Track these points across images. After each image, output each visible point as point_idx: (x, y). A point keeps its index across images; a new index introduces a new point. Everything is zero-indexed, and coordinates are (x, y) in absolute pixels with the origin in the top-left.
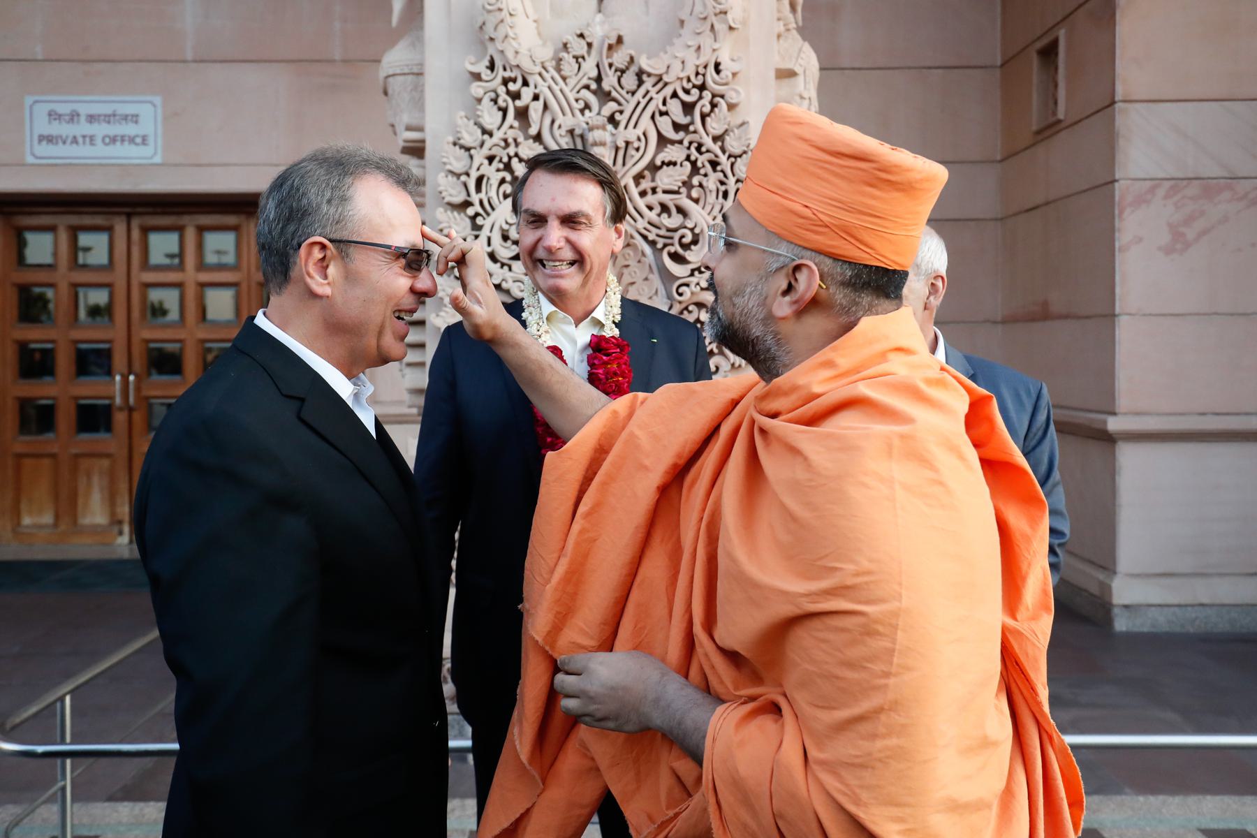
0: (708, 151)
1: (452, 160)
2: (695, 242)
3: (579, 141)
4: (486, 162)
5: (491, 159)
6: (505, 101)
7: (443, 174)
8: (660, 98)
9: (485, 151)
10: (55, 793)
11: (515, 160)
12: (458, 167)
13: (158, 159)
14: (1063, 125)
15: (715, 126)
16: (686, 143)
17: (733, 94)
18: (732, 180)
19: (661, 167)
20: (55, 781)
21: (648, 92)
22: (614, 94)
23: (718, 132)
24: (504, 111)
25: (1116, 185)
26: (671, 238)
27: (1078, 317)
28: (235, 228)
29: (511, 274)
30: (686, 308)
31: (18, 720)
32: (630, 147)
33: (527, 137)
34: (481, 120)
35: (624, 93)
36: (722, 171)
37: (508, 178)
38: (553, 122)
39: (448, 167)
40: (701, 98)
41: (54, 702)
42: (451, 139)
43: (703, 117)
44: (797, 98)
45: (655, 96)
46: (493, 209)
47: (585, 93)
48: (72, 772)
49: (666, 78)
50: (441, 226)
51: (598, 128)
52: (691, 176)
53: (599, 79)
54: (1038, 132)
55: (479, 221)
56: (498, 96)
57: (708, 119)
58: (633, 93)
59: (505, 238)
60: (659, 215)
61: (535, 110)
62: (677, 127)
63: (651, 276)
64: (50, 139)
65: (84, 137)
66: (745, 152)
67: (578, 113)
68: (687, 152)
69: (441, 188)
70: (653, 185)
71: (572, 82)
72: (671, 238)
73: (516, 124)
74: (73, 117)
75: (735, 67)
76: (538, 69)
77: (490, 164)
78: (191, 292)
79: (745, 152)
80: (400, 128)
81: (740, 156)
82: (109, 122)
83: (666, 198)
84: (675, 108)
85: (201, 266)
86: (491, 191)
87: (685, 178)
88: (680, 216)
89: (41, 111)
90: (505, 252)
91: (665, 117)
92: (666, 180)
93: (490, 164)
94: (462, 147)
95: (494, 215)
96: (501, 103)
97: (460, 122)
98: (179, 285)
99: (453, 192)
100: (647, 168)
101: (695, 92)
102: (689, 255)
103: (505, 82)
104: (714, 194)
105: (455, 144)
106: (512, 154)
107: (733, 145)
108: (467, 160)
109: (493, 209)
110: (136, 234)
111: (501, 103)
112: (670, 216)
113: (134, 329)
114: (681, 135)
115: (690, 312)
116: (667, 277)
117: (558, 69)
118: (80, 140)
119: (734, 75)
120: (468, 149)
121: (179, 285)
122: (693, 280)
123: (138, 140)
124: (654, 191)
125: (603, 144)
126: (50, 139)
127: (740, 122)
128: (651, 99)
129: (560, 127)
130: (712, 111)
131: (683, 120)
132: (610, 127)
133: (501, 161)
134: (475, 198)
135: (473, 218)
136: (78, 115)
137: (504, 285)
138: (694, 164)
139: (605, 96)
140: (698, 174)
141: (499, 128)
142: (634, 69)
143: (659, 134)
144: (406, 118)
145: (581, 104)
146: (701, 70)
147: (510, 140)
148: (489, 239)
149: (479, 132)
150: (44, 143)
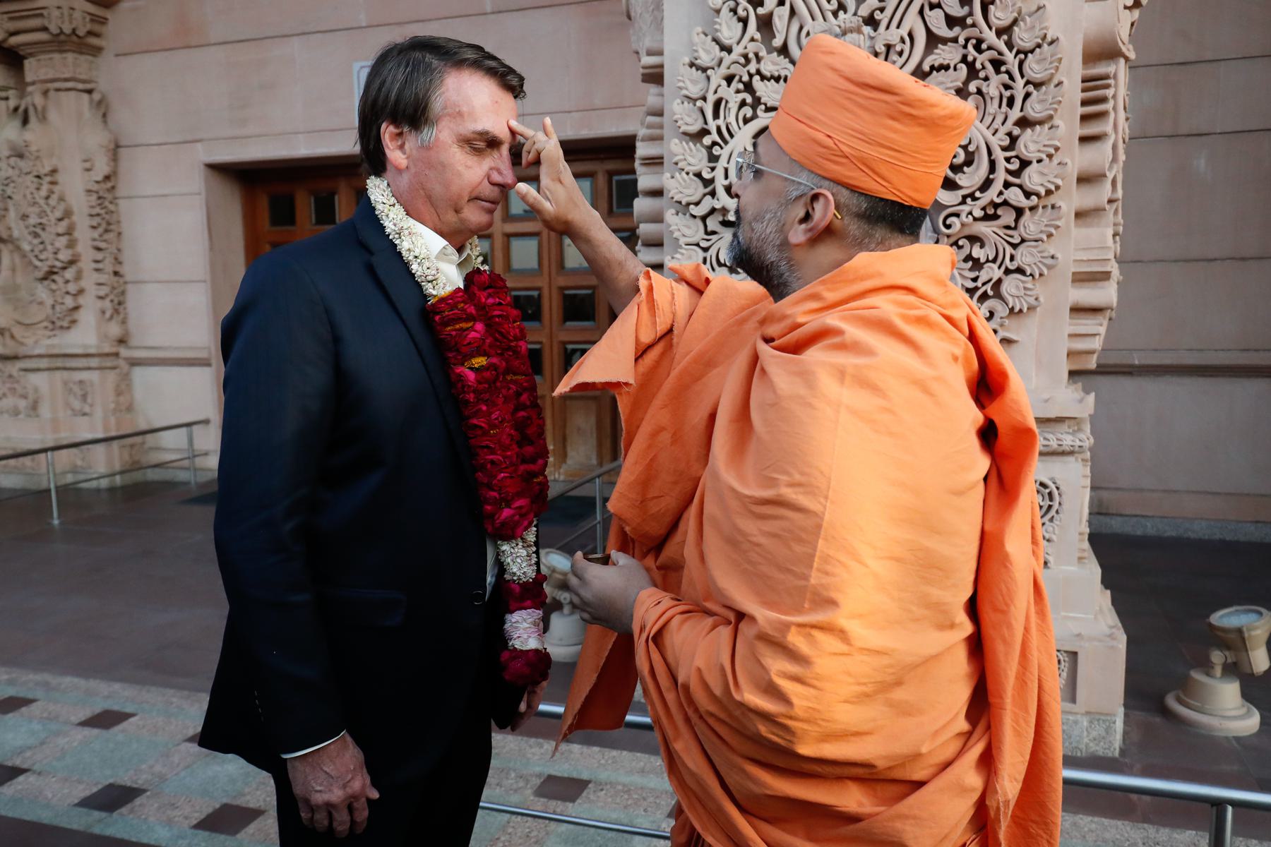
0: (990, 48)
2: (969, 162)
4: (724, 83)
5: (729, 79)
6: (746, 9)
7: (679, 101)
9: (723, 71)
11: (757, 78)
12: (694, 91)
15: (1000, 15)
16: (961, 40)
18: (1020, 82)
24: (744, 21)
33: (770, 50)
36: (1008, 72)
37: (749, 100)
38: (801, 28)
39: (685, 92)
42: (687, 60)
50: (676, 159)
52: (966, 83)
57: (992, 7)
61: (781, 18)
62: (951, 21)
66: (1039, 46)
67: (830, 16)
68: (964, 51)
69: (676, 117)
73: (758, 36)
77: (729, 86)
79: (1039, 46)
80: (643, 53)
81: (1032, 51)
86: (730, 116)
91: (938, 12)
93: (729, 86)
94: (698, 68)
95: (732, 143)
97: (696, 39)
99: (688, 120)
102: (960, 179)
104: (996, 102)
105: (692, 65)
106: (753, 71)
107: (1023, 37)
108: (703, 84)
111: (741, 12)
114: (957, 29)
115: (960, 247)
120: (704, 70)
122: (966, 208)
127: (1035, 8)
129: (808, 34)
131: (958, 11)
132: (867, 30)
134: (712, 125)
135: (709, 148)
138: (971, 66)
140: (978, 78)
144: (648, 43)
147: (751, 55)
148: (726, 170)
149: (717, 47)
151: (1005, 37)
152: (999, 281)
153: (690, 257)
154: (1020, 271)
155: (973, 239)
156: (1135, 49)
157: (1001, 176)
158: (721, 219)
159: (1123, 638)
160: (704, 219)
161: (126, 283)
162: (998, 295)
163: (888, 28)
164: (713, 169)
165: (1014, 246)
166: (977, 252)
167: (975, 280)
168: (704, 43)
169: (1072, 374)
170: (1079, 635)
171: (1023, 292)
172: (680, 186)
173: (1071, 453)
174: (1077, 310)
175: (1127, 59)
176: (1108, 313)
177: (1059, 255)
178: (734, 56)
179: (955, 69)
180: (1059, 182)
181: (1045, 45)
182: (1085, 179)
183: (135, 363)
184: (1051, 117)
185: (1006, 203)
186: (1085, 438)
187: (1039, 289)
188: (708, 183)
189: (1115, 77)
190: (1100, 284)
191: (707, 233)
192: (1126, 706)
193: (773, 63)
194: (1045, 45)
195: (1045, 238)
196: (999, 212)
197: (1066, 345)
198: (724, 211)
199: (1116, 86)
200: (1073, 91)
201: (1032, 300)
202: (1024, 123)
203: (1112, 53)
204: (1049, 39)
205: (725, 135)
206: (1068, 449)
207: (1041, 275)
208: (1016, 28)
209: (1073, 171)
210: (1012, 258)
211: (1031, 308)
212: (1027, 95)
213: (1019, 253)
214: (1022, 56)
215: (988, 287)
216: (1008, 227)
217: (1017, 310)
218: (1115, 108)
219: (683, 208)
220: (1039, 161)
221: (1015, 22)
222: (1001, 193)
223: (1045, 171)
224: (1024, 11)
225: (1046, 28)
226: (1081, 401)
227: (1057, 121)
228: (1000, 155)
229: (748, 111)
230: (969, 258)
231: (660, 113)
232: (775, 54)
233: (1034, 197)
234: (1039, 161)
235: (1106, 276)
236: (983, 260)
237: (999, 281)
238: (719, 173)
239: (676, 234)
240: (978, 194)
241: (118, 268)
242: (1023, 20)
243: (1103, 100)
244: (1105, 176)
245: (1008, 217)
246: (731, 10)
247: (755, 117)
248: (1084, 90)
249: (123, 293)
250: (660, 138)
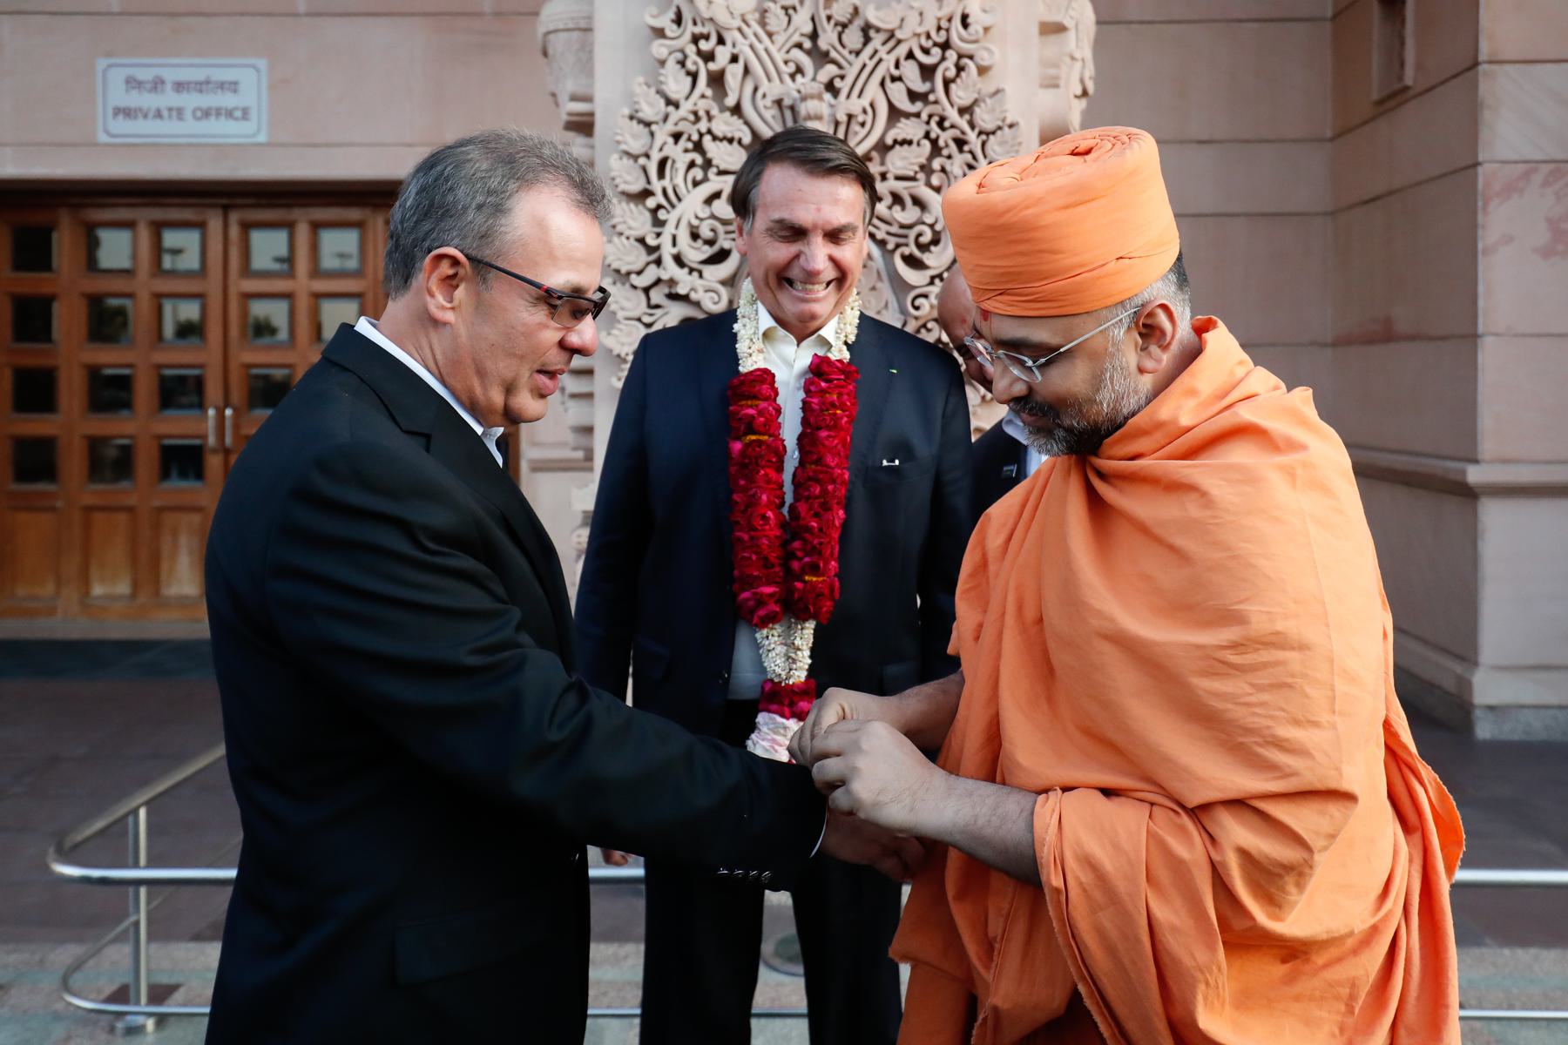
0: (952, 126)
1: (628, 138)
2: (936, 241)
3: (788, 114)
4: (671, 140)
5: (677, 137)
6: (695, 63)
8: (891, 59)
9: (670, 127)
10: (126, 931)
11: (707, 139)
12: (636, 146)
13: (262, 138)
14: (1411, 93)
15: (962, 95)
16: (924, 116)
17: (985, 54)
19: (892, 147)
20: (127, 915)
21: (876, 52)
22: (833, 54)
23: (966, 102)
24: (694, 76)
25: (1480, 170)
26: (906, 236)
27: (1431, 338)
28: (359, 225)
29: (700, 282)
30: (924, 326)
31: (79, 837)
33: (723, 109)
34: (664, 87)
35: (845, 52)
36: (971, 152)
38: (756, 89)
39: (623, 147)
40: (943, 59)
41: (126, 816)
42: (627, 112)
43: (947, 83)
44: (1067, 59)
45: (884, 56)
46: (679, 200)
47: (797, 53)
48: (148, 903)
49: (899, 35)
51: (812, 97)
53: (814, 36)
54: (1381, 102)
55: (662, 215)
56: (686, 57)
57: (953, 86)
58: (858, 53)
59: (695, 236)
60: (890, 208)
61: (733, 75)
62: (913, 96)
63: (879, 285)
64: (127, 113)
65: (170, 109)
66: (1000, 128)
67: (787, 79)
68: (925, 127)
69: (613, 174)
70: (882, 169)
71: (780, 39)
72: (906, 236)
73: (709, 92)
74: (157, 85)
75: (987, 20)
76: (737, 23)
78: (303, 304)
79: (1000, 128)
80: (563, 97)
81: (993, 133)
82: (201, 91)
83: (900, 186)
84: (911, 72)
85: (316, 272)
86: (678, 177)
87: (923, 160)
89: (117, 77)
90: (695, 254)
91: (898, 84)
92: (899, 163)
94: (640, 121)
95: (680, 207)
96: (690, 66)
98: (288, 296)
99: (629, 178)
101: (936, 51)
102: (927, 258)
103: (696, 39)
105: (631, 118)
106: (704, 130)
107: (985, 118)
108: (646, 139)
109: (679, 200)
110: (234, 231)
111: (690, 66)
112: (903, 208)
113: (233, 350)
114: (918, 106)
115: (929, 330)
116: (900, 286)
117: (763, 24)
118: (165, 113)
119: (986, 29)
120: (648, 124)
121: (288, 296)
123: (238, 114)
125: (819, 118)
126: (127, 113)
127: (992, 89)
128: (880, 60)
130: (958, 75)
131: (920, 87)
132: (828, 96)
133: (689, 139)
134: (657, 186)
136: (163, 82)
137: (693, 296)
138: (934, 142)
139: (821, 58)
140: (939, 154)
141: (687, 98)
142: (859, 23)
144: (570, 85)
145: (792, 68)
146: (944, 24)
147: (701, 113)
148: (674, 238)
149: (662, 102)
150: (121, 117)
151: (967, 117)
158: (667, 291)
160: (647, 290)
163: (848, 96)
164: (658, 235)
181: (1006, 129)
188: (651, 250)
191: (650, 306)
193: (724, 124)
194: (1006, 129)
198: (672, 282)
204: (1008, 121)
205: (673, 199)
214: (984, 137)
221: (976, 102)
229: (697, 173)
232: (728, 114)
238: (665, 240)
247: (706, 179)
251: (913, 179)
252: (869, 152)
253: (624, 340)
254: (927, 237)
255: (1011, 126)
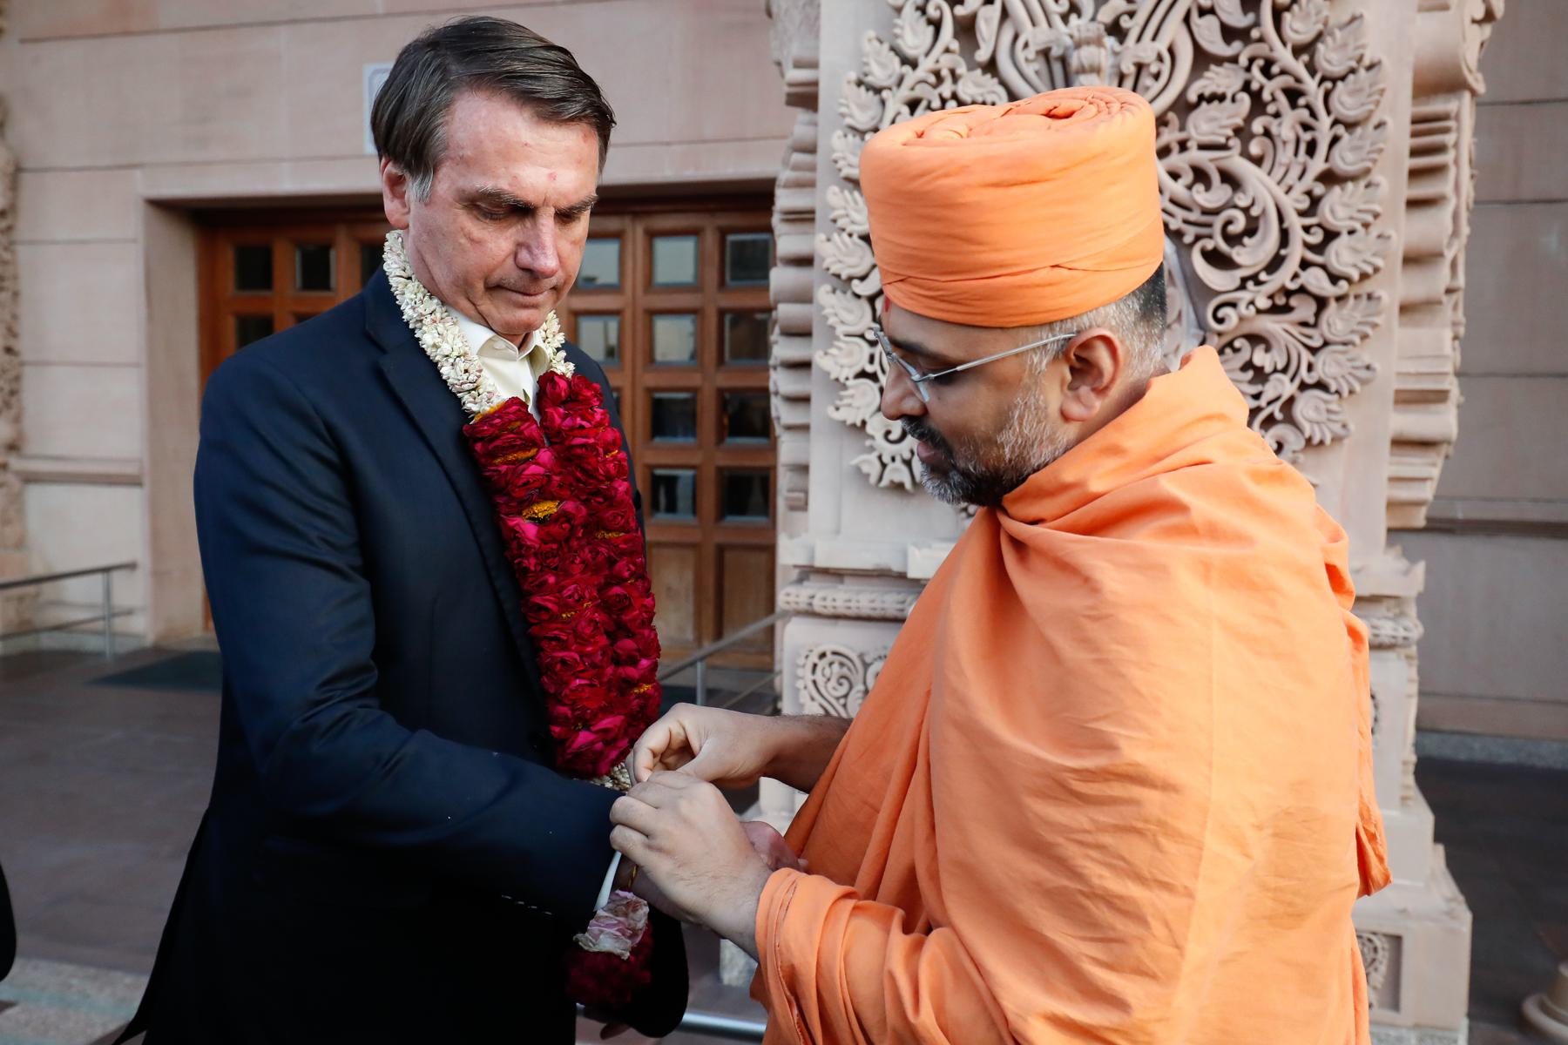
0: (1283, 72)
2: (1251, 231)
3: (1057, 68)
4: (906, 110)
6: (939, 8)
7: (840, 133)
9: (905, 93)
15: (1299, 27)
16: (1243, 61)
18: (1325, 121)
19: (1194, 107)
23: (1305, 37)
24: (937, 25)
26: (1209, 225)
30: (1230, 344)
32: (1144, 73)
34: (899, 42)
36: (1308, 107)
38: (1016, 37)
39: (849, 121)
42: (853, 76)
50: (833, 215)
51: (1088, 42)
52: (1249, 119)
57: (1287, 16)
60: (1189, 187)
62: (1229, 33)
66: (1353, 71)
67: (1057, 21)
68: (1245, 76)
69: (835, 156)
70: (1182, 136)
72: (1209, 225)
73: (955, 45)
77: (912, 112)
79: (1353, 71)
81: (1343, 78)
83: (1204, 158)
87: (1239, 121)
88: (1227, 189)
91: (1210, 20)
92: (1205, 127)
93: (912, 112)
94: (869, 88)
96: (932, 12)
97: (867, 47)
100: (1173, 107)
102: (1237, 254)
104: (1291, 148)
105: (860, 83)
106: (947, 94)
107: (1330, 58)
108: (875, 109)
111: (932, 12)
112: (1208, 187)
114: (1237, 45)
115: (1236, 350)
120: (878, 91)
122: (1244, 296)
124: (1183, 146)
125: (1096, 70)
127: (1346, 18)
129: (1026, 45)
131: (1238, 20)
132: (1110, 41)
138: (1256, 97)
140: (1264, 113)
141: (927, 54)
143: (1197, 48)
144: (795, 50)
147: (945, 73)
149: (897, 60)
151: (1305, 58)
152: (1291, 400)
153: (850, 354)
154: (1321, 386)
155: (1255, 339)
156: (1486, 80)
157: (1296, 252)
159: (1467, 917)
160: (872, 300)
161: (22, 364)
162: (1289, 419)
163: (1139, 39)
165: (1314, 351)
166: (1260, 358)
167: (1257, 397)
168: (878, 53)
169: (1390, 530)
170: (1403, 911)
171: (1324, 416)
172: (838, 252)
173: (1390, 647)
174: (1401, 443)
175: (1473, 93)
176: (1444, 449)
177: (1377, 365)
178: (921, 73)
179: (1233, 100)
180: (1379, 262)
181: (1362, 72)
182: (1414, 260)
183: (30, 479)
184: (1367, 171)
185: (1302, 290)
186: (1412, 627)
187: (1347, 412)
189: (1457, 118)
190: (1433, 407)
192: (1470, 1016)
194: (1362, 72)
195: (1356, 339)
196: (1293, 302)
197: (1385, 492)
199: (1459, 130)
200: (1399, 136)
201: (1337, 428)
202: (1329, 178)
203: (1452, 84)
204: (1367, 62)
206: (1387, 641)
207: (1351, 392)
208: (1320, 47)
209: (1398, 247)
210: (1310, 367)
211: (1337, 439)
212: (1335, 140)
213: (1320, 360)
214: (1329, 85)
215: (1275, 409)
216: (1304, 324)
217: (1316, 440)
218: (1456, 162)
219: (843, 283)
220: (1351, 232)
221: (1319, 37)
222: (1296, 276)
223: (1360, 246)
224: (1332, 22)
225: (1363, 47)
226: (1406, 573)
227: (1376, 177)
228: (1295, 223)
230: (1248, 366)
231: (812, 150)
232: (979, 71)
233: (1343, 283)
234: (1351, 232)
235: (1440, 396)
236: (1268, 369)
237: (1291, 400)
239: (832, 321)
240: (1263, 276)
241: (12, 343)
242: (1332, 34)
243: (1439, 149)
244: (1440, 255)
245: (1304, 309)
246: (918, 8)
248: (1414, 135)
249: (17, 378)
250: (811, 184)
251: (1224, 147)
252: (1164, 113)
253: (844, 361)
254: (1240, 224)
255: (1370, 68)
